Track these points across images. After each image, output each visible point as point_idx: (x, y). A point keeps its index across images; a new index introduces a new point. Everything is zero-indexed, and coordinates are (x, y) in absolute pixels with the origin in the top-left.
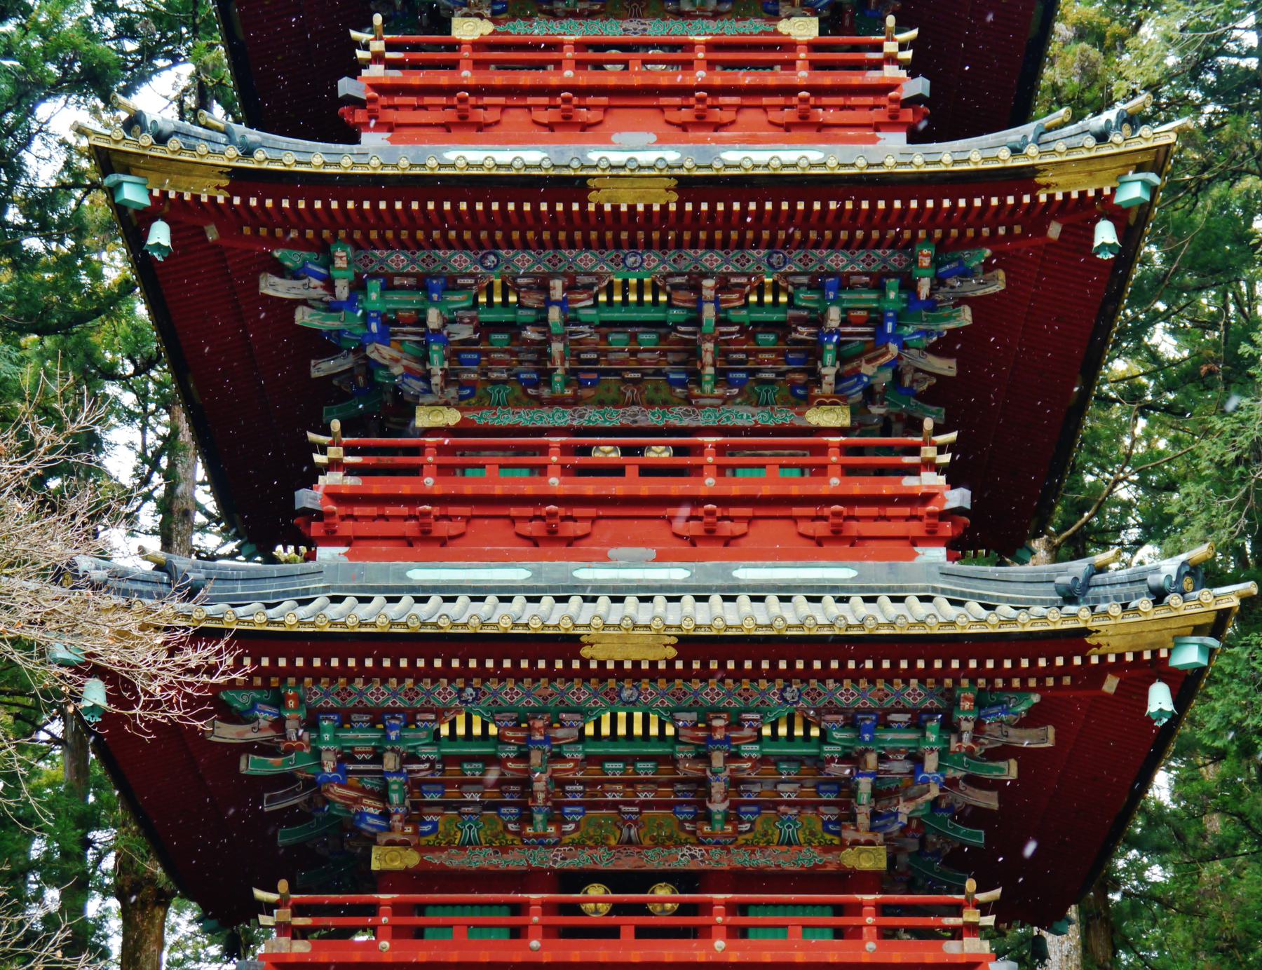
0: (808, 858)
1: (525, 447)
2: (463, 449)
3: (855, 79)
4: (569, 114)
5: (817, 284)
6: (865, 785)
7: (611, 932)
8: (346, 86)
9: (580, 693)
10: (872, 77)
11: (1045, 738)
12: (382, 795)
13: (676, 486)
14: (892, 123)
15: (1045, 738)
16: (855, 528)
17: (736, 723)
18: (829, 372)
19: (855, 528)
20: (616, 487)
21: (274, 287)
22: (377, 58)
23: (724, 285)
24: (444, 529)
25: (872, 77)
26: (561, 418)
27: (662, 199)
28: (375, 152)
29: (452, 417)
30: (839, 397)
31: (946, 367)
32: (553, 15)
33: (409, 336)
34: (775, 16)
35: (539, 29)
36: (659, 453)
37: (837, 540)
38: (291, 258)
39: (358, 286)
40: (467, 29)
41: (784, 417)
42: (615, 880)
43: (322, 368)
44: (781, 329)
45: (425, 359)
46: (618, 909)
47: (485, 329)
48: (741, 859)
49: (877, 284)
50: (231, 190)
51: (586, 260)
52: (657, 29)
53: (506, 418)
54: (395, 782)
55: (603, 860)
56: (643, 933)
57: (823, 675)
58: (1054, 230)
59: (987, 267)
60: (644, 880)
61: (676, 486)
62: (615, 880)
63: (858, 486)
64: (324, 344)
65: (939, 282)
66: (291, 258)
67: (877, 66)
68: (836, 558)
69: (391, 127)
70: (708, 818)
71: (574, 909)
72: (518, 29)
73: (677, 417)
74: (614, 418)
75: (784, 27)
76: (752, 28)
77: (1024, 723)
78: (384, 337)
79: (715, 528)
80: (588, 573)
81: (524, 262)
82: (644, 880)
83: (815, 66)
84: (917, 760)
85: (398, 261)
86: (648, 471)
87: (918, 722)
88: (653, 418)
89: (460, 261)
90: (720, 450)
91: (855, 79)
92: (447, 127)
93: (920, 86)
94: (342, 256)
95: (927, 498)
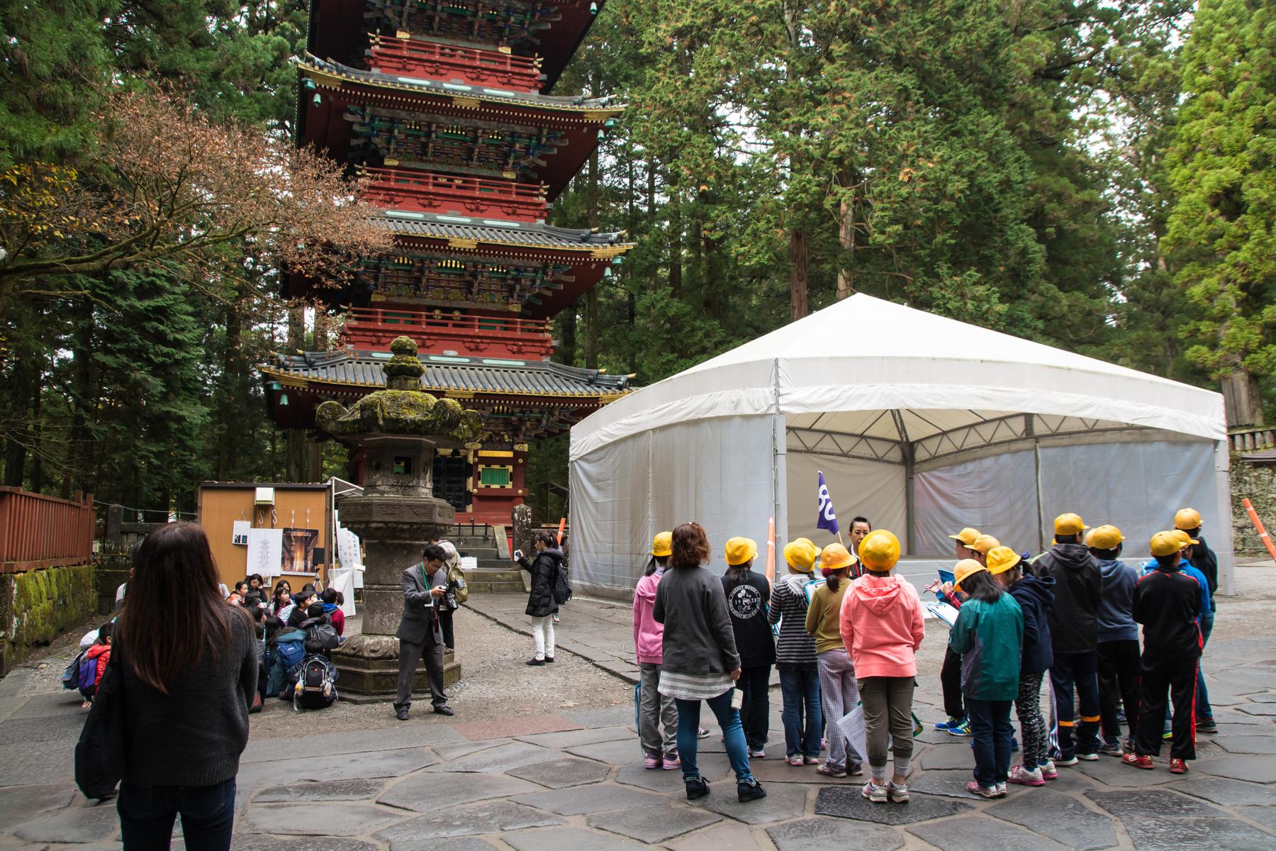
0: (498, 307)
1: (419, 175)
2: (402, 175)
3: (525, 71)
4: (437, 69)
5: (513, 134)
6: (518, 287)
7: (446, 325)
8: (367, 52)
9: (438, 254)
10: (529, 71)
11: (573, 279)
12: (376, 279)
13: (468, 193)
14: (535, 87)
15: (573, 279)
16: (519, 211)
17: (484, 267)
18: (511, 162)
19: (519, 211)
20: (449, 191)
21: (348, 117)
22: (377, 43)
23: (484, 132)
24: (397, 199)
25: (529, 71)
26: (429, 167)
27: (475, 106)
28: (376, 77)
29: (396, 163)
30: (513, 169)
31: (543, 163)
32: (429, 35)
33: (385, 135)
34: (497, 45)
35: (425, 39)
36: (458, 182)
37: (512, 215)
38: (353, 108)
39: (373, 118)
40: (402, 35)
41: (496, 174)
42: (444, 310)
43: (354, 142)
44: (498, 146)
45: (389, 143)
46: (443, 318)
47: (408, 135)
48: (484, 307)
49: (530, 137)
50: (342, 87)
51: (442, 119)
52: (462, 44)
53: (413, 165)
54: (381, 276)
55: (440, 303)
56: (454, 325)
57: (509, 256)
58: (585, 130)
59: (563, 137)
60: (451, 310)
61: (468, 193)
62: (444, 310)
63: (521, 199)
64: (357, 135)
65: (548, 139)
66: (353, 108)
67: (531, 68)
68: (514, 221)
69: (381, 67)
70: (471, 293)
71: (431, 317)
72: (418, 38)
73: (464, 170)
74: (446, 169)
75: (501, 49)
76: (491, 48)
77: (566, 273)
78: (377, 136)
79: (476, 206)
80: (440, 218)
81: (423, 116)
82: (451, 310)
83: (512, 65)
84: (534, 281)
85: (383, 112)
86: (459, 187)
87: (536, 271)
88: (457, 170)
89: (403, 114)
90: (481, 183)
91: (525, 71)
92: (399, 69)
93: (544, 77)
94: (368, 110)
95: (540, 204)
